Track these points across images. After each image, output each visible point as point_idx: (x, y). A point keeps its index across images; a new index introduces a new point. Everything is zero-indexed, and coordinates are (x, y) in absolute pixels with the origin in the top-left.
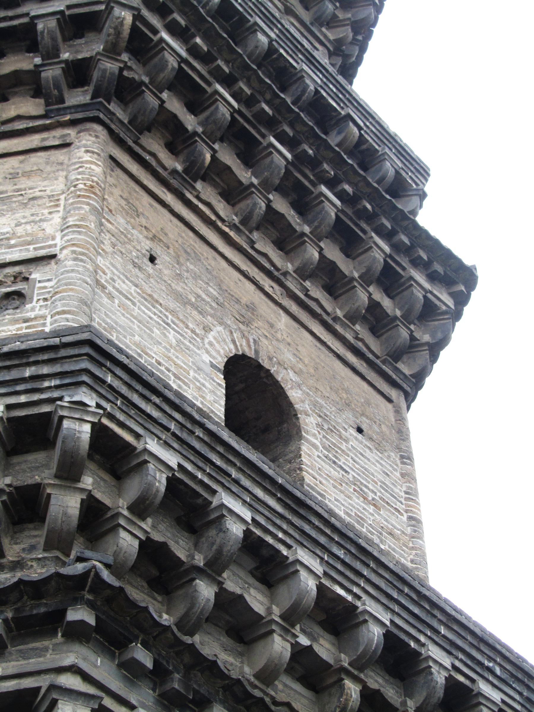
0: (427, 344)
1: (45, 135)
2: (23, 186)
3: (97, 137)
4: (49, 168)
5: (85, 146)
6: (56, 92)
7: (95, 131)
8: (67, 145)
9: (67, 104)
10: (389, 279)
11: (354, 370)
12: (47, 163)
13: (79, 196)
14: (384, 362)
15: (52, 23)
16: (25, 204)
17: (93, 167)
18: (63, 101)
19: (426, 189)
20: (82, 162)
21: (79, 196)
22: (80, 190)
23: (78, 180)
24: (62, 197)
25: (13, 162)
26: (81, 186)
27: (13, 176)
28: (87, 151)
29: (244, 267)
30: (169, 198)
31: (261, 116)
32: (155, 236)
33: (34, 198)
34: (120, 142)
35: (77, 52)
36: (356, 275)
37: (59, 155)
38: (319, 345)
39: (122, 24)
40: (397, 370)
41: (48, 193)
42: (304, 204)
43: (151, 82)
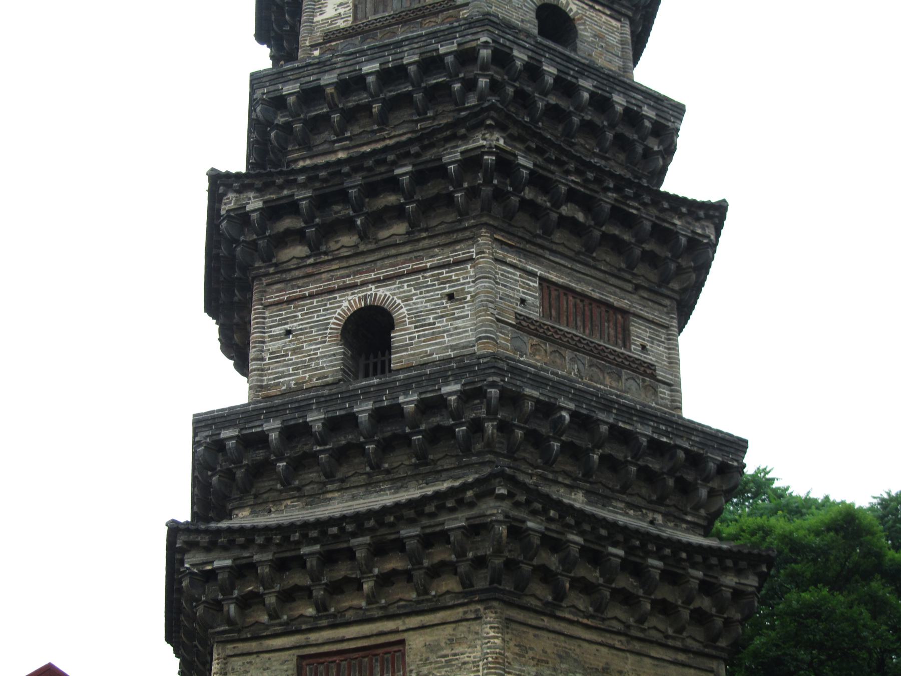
0: (738, 621)
1: (465, 609)
2: (457, 651)
3: (496, 613)
4: (471, 637)
5: (490, 623)
6: (468, 582)
7: (494, 608)
8: (478, 618)
9: (476, 588)
10: (708, 588)
11: (683, 665)
12: (469, 632)
13: (490, 668)
14: (706, 646)
15: (459, 532)
16: (460, 668)
17: (496, 641)
18: (472, 586)
19: (745, 461)
20: (489, 638)
21: (490, 668)
22: (490, 663)
23: (488, 653)
24: (481, 663)
25: (449, 629)
26: (490, 659)
27: (451, 642)
28: (491, 628)
29: (599, 639)
30: (546, 622)
31: (601, 538)
32: (538, 661)
33: (464, 663)
34: (511, 605)
35: (477, 549)
36: (679, 603)
37: (475, 626)
38: (656, 663)
39: (501, 537)
40: (716, 648)
41: (472, 659)
42: (637, 571)
43: (525, 558)
